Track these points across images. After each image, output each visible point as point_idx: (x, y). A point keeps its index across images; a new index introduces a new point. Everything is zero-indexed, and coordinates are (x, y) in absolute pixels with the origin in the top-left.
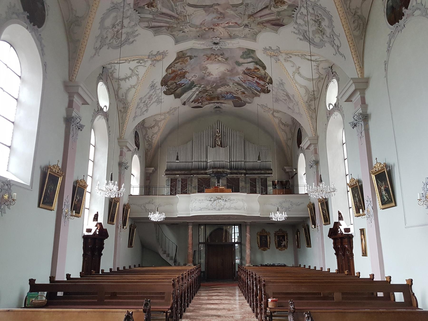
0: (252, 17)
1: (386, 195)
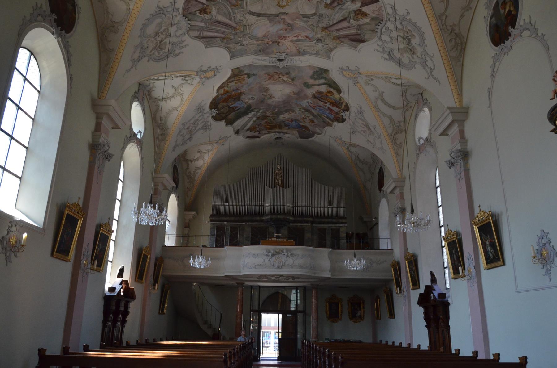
0: (326, 30)
1: (491, 251)
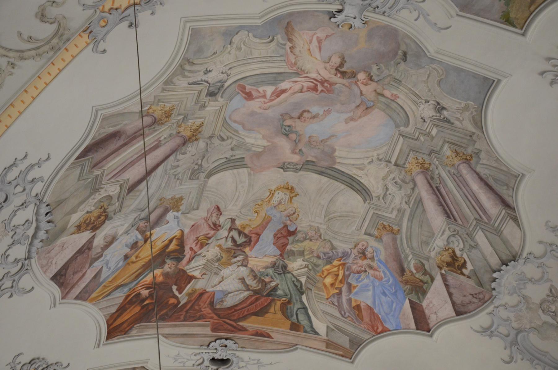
0: (188, 134)
